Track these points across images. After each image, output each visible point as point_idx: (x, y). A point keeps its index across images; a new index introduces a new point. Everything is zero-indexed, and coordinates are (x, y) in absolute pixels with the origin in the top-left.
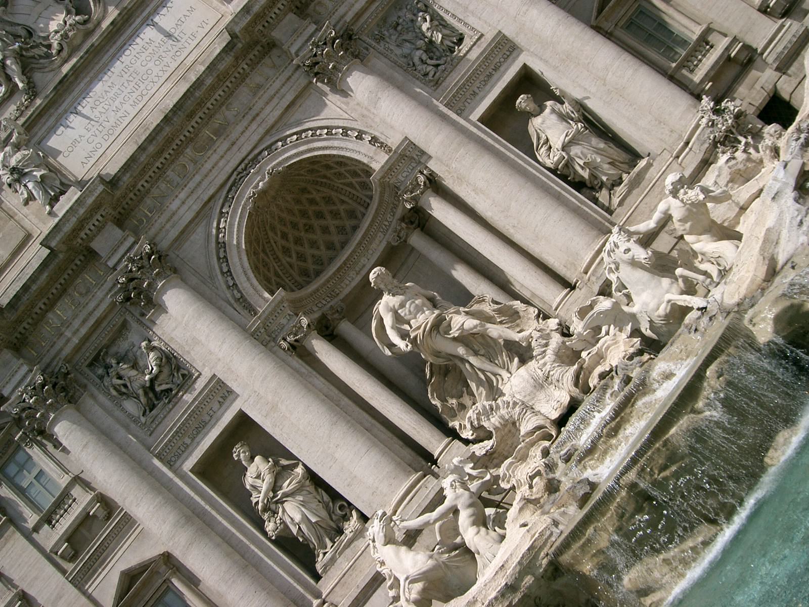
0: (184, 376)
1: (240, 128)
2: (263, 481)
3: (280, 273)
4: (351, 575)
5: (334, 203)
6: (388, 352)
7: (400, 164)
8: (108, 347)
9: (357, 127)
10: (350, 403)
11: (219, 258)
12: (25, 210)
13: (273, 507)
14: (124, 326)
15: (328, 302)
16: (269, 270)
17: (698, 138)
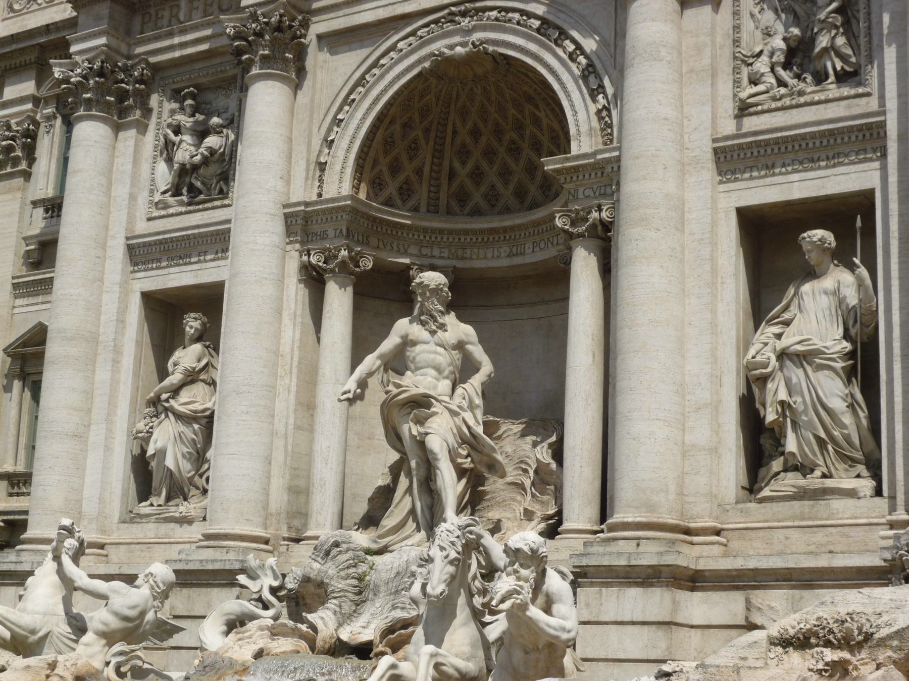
0: (221, 191)
4: (142, 551)
7: (593, 175)
10: (294, 389)
13: (160, 409)
15: (441, 257)
16: (411, 159)
17: (897, 537)
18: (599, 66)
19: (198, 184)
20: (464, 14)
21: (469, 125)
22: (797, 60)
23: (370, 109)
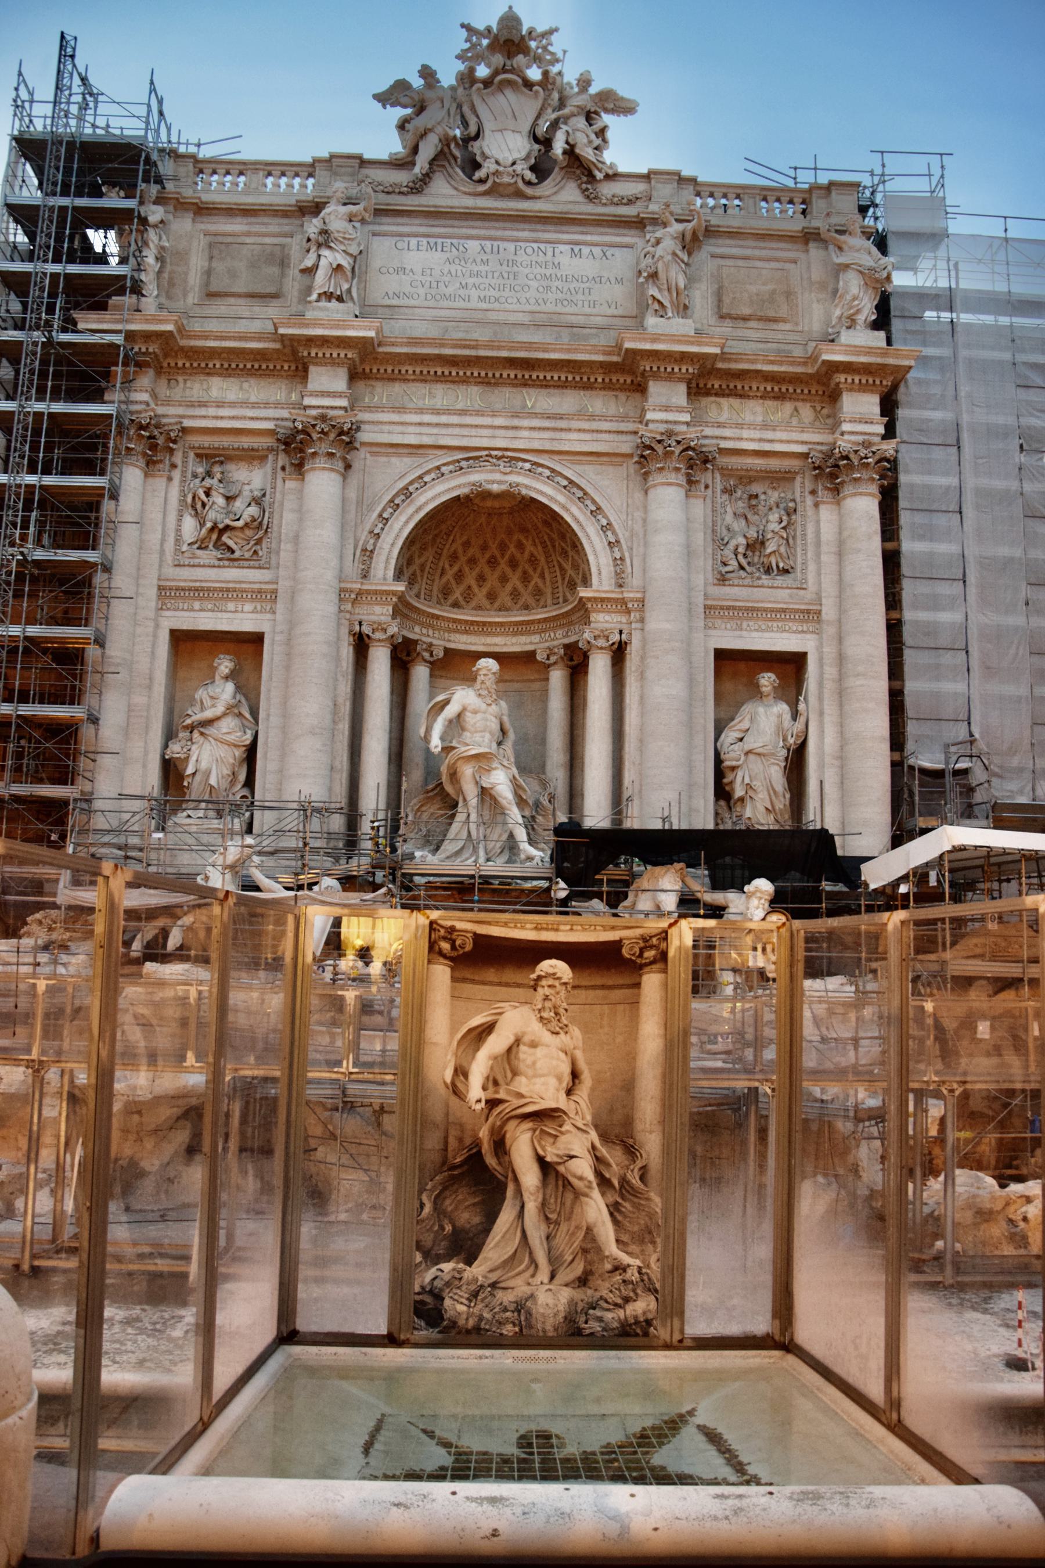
0: (255, 552)
1: (536, 423)
2: (213, 706)
3: (427, 569)
5: (535, 569)
6: (422, 732)
8: (229, 458)
9: (621, 536)
11: (392, 501)
12: (297, 272)
14: (263, 458)
18: (616, 527)
19: (231, 543)
20: (499, 458)
21: (465, 538)
22: (749, 553)
23: (412, 515)
